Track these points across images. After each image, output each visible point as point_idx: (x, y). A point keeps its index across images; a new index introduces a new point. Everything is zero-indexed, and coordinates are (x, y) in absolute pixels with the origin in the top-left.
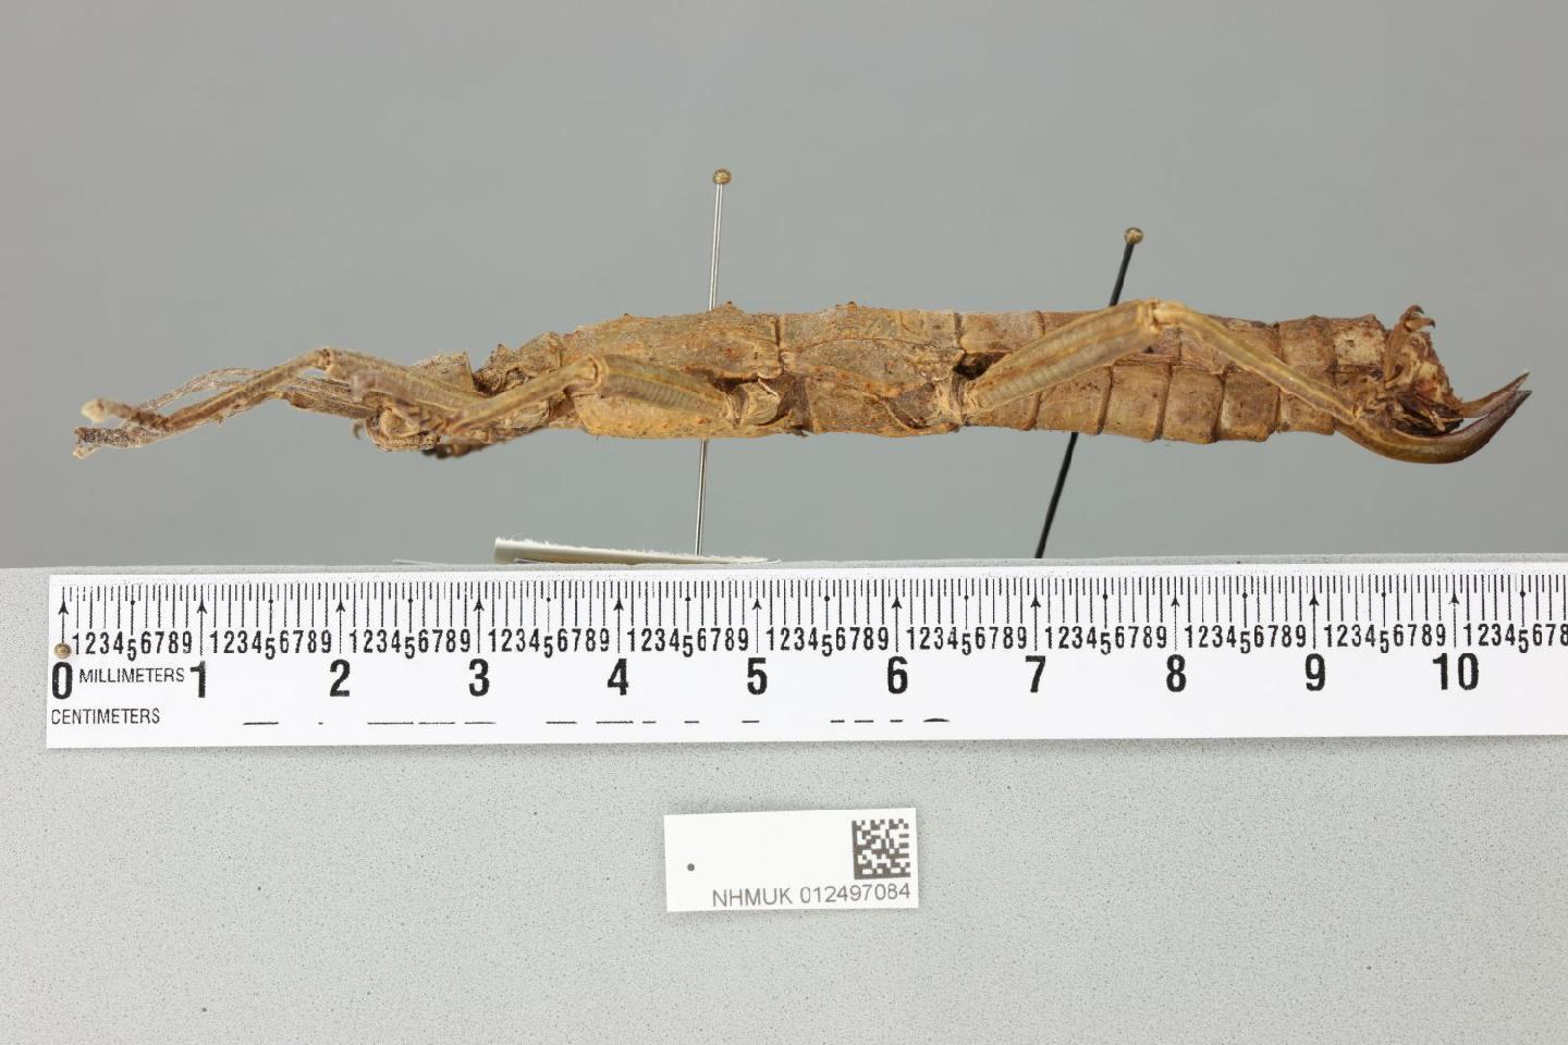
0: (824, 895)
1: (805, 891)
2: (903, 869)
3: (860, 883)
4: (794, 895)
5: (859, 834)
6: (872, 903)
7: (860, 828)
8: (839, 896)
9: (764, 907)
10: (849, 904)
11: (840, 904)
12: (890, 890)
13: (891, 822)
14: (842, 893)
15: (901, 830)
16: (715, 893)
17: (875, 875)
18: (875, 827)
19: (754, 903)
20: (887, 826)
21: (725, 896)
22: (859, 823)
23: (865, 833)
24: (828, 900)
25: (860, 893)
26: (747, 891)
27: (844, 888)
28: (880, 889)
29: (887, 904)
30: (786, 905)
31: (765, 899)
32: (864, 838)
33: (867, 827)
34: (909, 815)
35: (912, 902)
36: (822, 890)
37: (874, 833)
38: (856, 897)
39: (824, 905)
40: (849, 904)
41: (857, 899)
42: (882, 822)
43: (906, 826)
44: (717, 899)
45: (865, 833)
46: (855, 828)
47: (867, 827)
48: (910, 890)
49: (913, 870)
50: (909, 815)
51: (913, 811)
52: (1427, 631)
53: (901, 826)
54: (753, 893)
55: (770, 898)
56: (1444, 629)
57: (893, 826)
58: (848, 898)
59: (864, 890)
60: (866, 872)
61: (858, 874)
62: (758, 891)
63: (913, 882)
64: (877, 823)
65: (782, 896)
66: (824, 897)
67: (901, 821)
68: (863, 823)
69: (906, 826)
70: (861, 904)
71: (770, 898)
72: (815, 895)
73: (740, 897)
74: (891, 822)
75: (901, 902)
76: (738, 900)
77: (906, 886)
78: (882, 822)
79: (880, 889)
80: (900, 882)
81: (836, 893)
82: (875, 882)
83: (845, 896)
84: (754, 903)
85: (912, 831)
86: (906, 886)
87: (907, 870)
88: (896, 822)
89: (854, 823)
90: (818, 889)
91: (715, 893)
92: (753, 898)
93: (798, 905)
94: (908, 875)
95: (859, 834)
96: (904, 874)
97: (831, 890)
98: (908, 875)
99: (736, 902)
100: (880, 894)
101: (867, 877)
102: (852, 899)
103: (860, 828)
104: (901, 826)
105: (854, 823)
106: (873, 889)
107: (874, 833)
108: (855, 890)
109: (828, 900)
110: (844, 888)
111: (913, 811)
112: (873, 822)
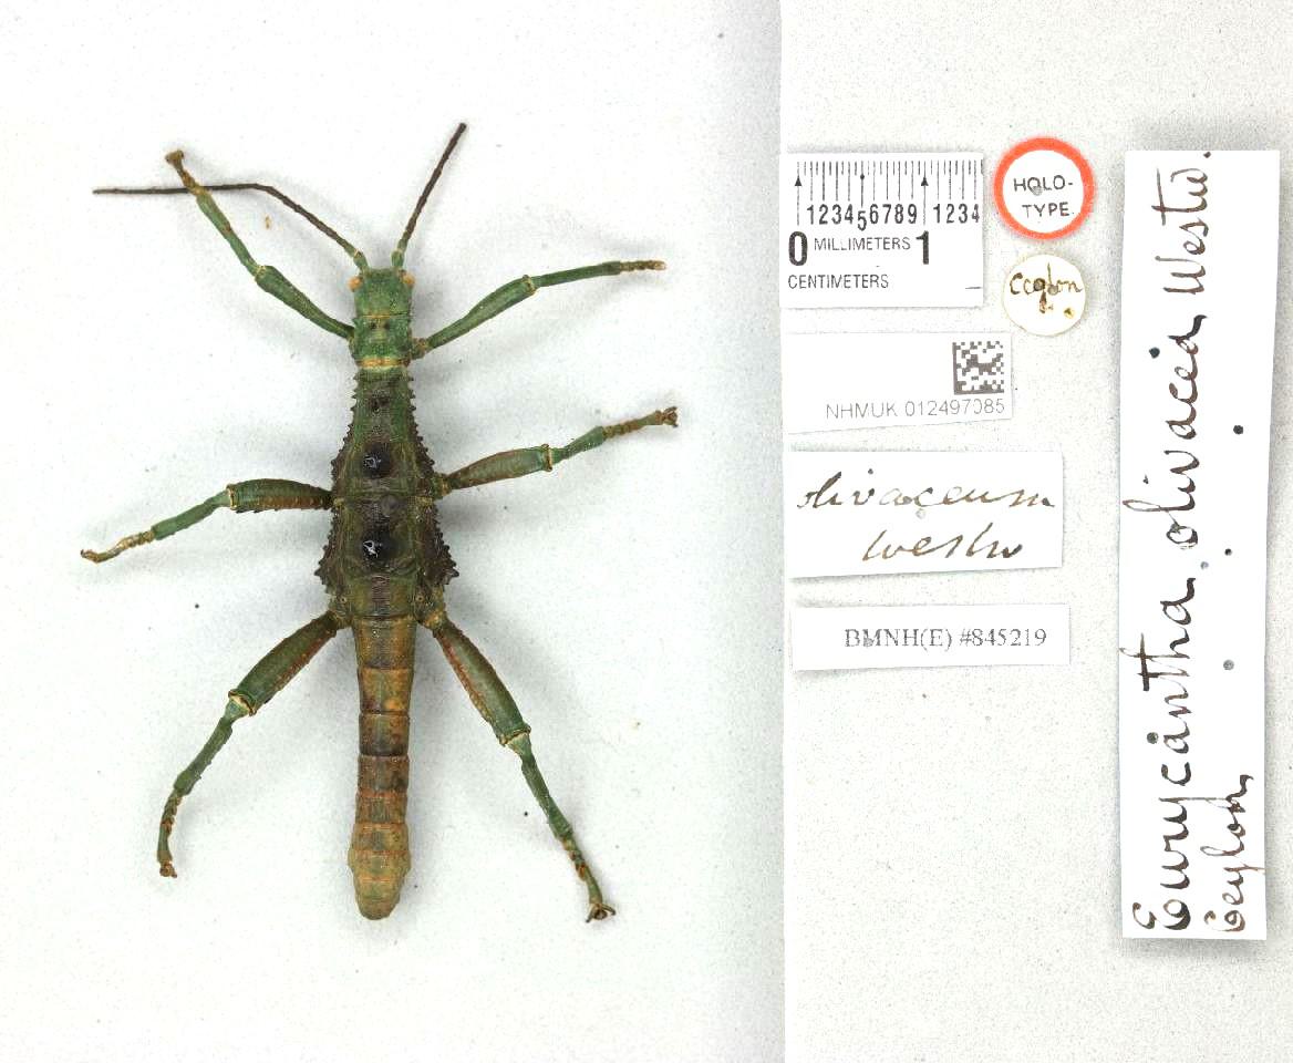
0: (927, 409)
4: (899, 408)
5: (959, 353)
7: (959, 348)
10: (950, 417)
20: (984, 346)
23: (965, 353)
32: (963, 356)
33: (967, 347)
37: (973, 352)
38: (955, 411)
45: (965, 353)
46: (955, 347)
47: (967, 347)
53: (997, 346)
57: (990, 346)
61: (958, 387)
72: (918, 409)
80: (994, 397)
81: (939, 406)
82: (972, 397)
88: (992, 344)
94: (1003, 391)
95: (959, 353)
96: (1000, 390)
97: (933, 405)
101: (968, 392)
103: (959, 348)
105: (954, 344)
107: (973, 352)
108: (955, 405)
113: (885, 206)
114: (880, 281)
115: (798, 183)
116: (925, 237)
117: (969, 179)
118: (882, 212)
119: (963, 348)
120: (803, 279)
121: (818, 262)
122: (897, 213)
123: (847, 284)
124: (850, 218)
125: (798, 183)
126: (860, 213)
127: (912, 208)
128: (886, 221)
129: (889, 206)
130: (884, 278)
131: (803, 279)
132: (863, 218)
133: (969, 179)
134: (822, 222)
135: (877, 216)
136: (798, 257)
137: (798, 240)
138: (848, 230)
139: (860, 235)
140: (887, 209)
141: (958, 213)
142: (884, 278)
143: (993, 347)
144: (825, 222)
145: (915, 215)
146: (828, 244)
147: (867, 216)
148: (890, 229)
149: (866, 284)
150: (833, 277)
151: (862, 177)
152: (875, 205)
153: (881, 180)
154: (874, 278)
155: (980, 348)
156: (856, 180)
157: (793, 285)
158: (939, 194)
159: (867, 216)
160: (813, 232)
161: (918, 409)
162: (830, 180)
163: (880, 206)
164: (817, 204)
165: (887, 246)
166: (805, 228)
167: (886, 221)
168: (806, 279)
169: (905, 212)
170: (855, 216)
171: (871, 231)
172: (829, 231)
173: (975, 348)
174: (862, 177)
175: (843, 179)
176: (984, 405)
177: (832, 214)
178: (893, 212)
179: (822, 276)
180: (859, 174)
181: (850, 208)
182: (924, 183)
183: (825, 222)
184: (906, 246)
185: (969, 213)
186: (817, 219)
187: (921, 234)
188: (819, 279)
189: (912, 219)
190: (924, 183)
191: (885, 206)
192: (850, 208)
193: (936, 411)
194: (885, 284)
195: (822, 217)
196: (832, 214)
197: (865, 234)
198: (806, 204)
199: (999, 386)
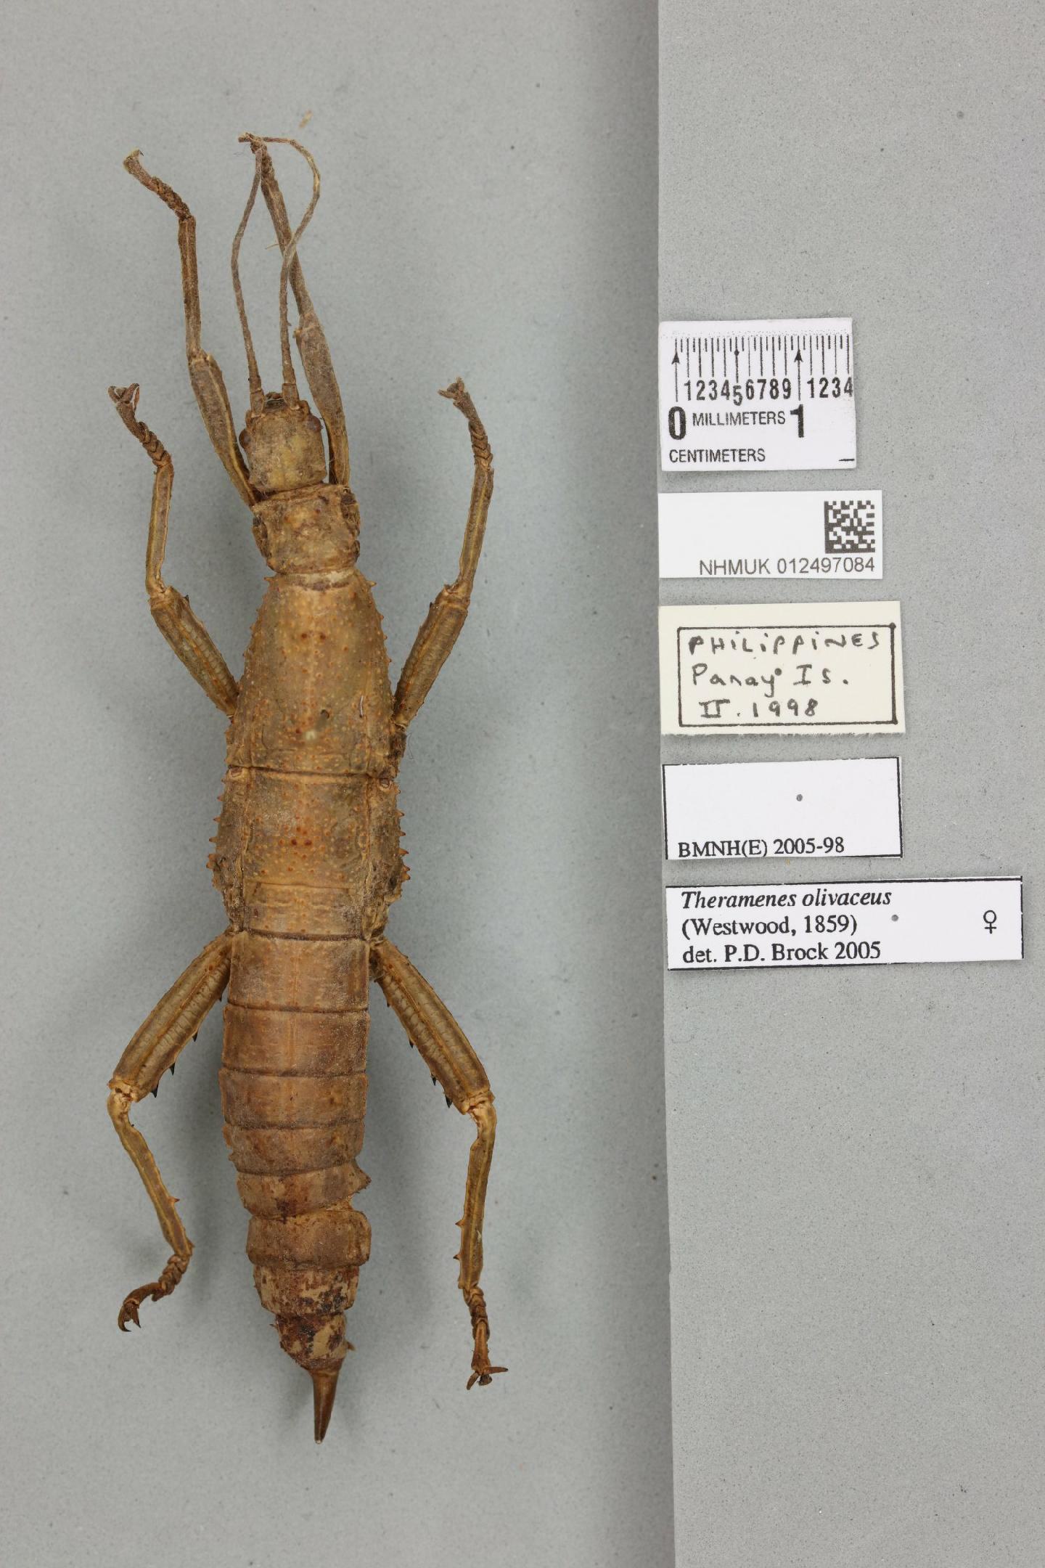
0: (799, 566)
1: (782, 562)
2: (869, 545)
3: (831, 556)
4: (772, 566)
5: (831, 513)
6: (841, 574)
8: (812, 568)
9: (745, 575)
11: (813, 574)
12: (857, 564)
13: (860, 503)
14: (815, 565)
15: (869, 510)
16: (702, 563)
17: (844, 550)
18: (844, 506)
19: (735, 573)
20: (855, 506)
21: (711, 565)
22: (830, 504)
23: (836, 512)
24: (801, 572)
25: (830, 565)
27: (817, 560)
28: (848, 562)
29: (854, 575)
30: (764, 574)
31: (746, 569)
32: (835, 517)
33: (838, 507)
34: (875, 497)
35: (877, 573)
37: (844, 512)
38: (826, 569)
40: (821, 575)
41: (827, 571)
42: (852, 503)
43: (873, 507)
44: (703, 567)
45: (836, 512)
46: (827, 507)
47: (838, 507)
48: (874, 564)
49: (878, 546)
52: (774, 386)
53: (868, 507)
54: (735, 565)
55: (751, 569)
56: (789, 383)
57: (861, 506)
58: (820, 570)
59: (834, 563)
60: (837, 547)
61: (829, 547)
62: (740, 562)
63: (878, 556)
64: (847, 503)
65: (760, 567)
66: (798, 569)
67: (868, 503)
68: (835, 503)
69: (873, 507)
70: (831, 575)
71: (751, 569)
72: (790, 566)
73: (724, 567)
74: (860, 503)
75: (867, 574)
76: (723, 569)
77: (871, 559)
78: (852, 503)
79: (848, 562)
80: (866, 557)
82: (843, 556)
83: (818, 568)
84: (735, 573)
85: (878, 511)
86: (871, 559)
87: (872, 546)
88: (864, 503)
89: (826, 504)
91: (702, 563)
92: (735, 568)
93: (775, 574)
94: (873, 550)
95: (831, 513)
96: (870, 549)
97: (804, 563)
98: (873, 550)
100: (848, 567)
102: (823, 571)
103: (831, 507)
105: (826, 504)
106: (842, 561)
107: (844, 512)
108: (826, 563)
109: (801, 572)
110: (817, 560)
112: (843, 503)
113: (759, 381)
115: (676, 360)
116: (799, 412)
119: (835, 507)
120: (682, 453)
121: (697, 437)
123: (726, 458)
124: (727, 395)
125: (676, 360)
128: (762, 397)
129: (764, 381)
130: (761, 452)
131: (682, 453)
132: (739, 394)
134: (700, 398)
137: (677, 415)
138: (723, 406)
139: (736, 410)
140: (761, 384)
141: (831, 387)
142: (761, 452)
143: (864, 507)
146: (704, 419)
148: (767, 404)
149: (743, 458)
150: (711, 451)
151: (737, 353)
152: (750, 381)
153: (755, 355)
154: (751, 452)
155: (852, 508)
156: (731, 356)
157: (674, 459)
159: (743, 391)
160: (691, 408)
161: (790, 566)
162: (706, 357)
163: (755, 381)
166: (683, 403)
167: (762, 397)
168: (686, 453)
169: (780, 387)
170: (731, 391)
171: (747, 405)
173: (847, 508)
174: (737, 353)
175: (719, 356)
176: (854, 564)
178: (768, 387)
179: (701, 451)
180: (734, 349)
181: (727, 383)
182: (798, 358)
186: (694, 395)
187: (796, 407)
188: (698, 454)
190: (798, 358)
191: (759, 381)
192: (727, 383)
193: (808, 569)
194: (761, 458)
195: (700, 393)
197: (741, 409)
198: (683, 379)
199: (869, 545)
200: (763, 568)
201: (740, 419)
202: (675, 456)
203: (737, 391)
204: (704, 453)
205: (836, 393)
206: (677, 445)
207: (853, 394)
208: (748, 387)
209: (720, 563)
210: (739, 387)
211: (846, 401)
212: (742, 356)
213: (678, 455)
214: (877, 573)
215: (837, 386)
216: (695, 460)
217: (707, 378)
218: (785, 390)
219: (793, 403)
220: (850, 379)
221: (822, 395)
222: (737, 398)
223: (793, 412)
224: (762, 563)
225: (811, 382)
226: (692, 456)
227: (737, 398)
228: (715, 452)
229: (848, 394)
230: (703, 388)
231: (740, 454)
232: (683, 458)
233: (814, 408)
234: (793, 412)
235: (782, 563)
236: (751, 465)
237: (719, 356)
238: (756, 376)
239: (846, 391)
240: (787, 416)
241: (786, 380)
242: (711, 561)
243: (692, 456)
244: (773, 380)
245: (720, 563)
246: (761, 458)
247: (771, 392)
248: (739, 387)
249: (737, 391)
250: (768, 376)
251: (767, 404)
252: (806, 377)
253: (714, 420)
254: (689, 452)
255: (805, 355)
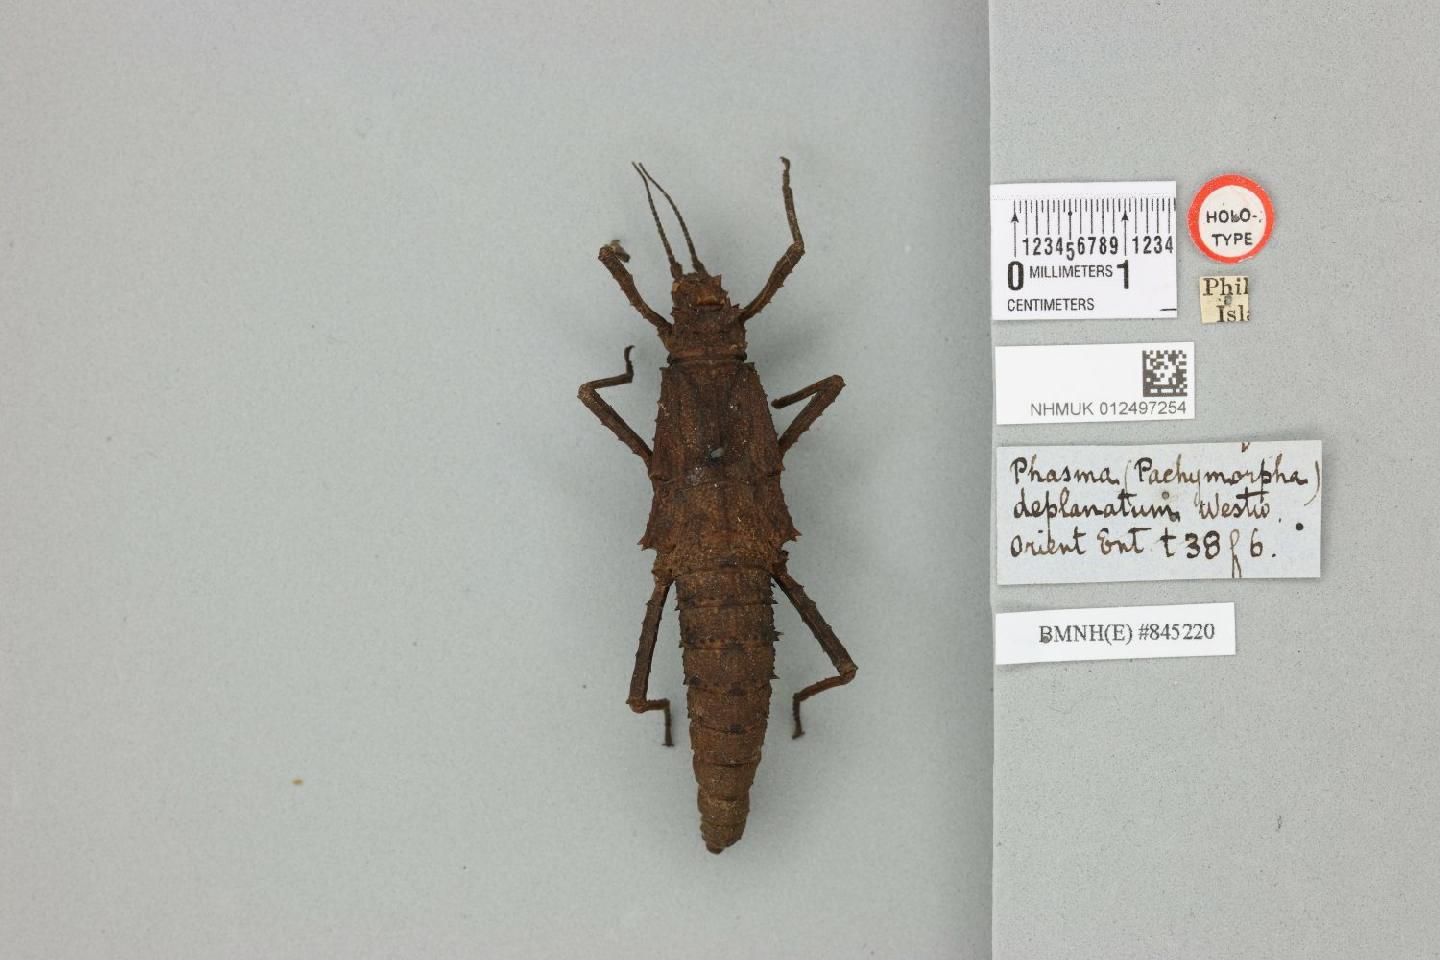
0: (1119, 409)
1: (1104, 406)
2: (1182, 390)
3: (1148, 399)
4: (1095, 408)
5: (1148, 361)
6: (1153, 415)
7: (1148, 357)
8: (1130, 410)
11: (1131, 416)
18: (1160, 356)
19: (1062, 414)
23: (1152, 361)
24: (1121, 413)
26: (1058, 405)
27: (1134, 404)
30: (1087, 418)
32: (1151, 364)
33: (1154, 356)
34: (1188, 348)
36: (1117, 406)
39: (1119, 418)
40: (1138, 417)
43: (1184, 356)
45: (1152, 361)
46: (1145, 356)
47: (1154, 356)
50: (1188, 348)
51: (1191, 345)
53: (1180, 356)
54: (1062, 407)
59: (1150, 406)
61: (1147, 393)
62: (1067, 405)
63: (1190, 401)
64: (1162, 353)
66: (1118, 411)
67: (1181, 352)
68: (1152, 353)
69: (1184, 356)
70: (1147, 417)
71: (1076, 411)
72: (1111, 409)
75: (1179, 415)
77: (1183, 403)
80: (1179, 400)
82: (1158, 399)
83: (1135, 410)
84: (1062, 414)
86: (1183, 403)
87: (1185, 391)
89: (1144, 353)
90: (1114, 405)
93: (1098, 417)
94: (1185, 394)
95: (1148, 361)
97: (1124, 406)
98: (1185, 394)
99: (1049, 412)
103: (1148, 357)
104: (1180, 356)
105: (1144, 353)
107: (1159, 360)
108: (1143, 406)
109: (1121, 413)
110: (1134, 404)
111: (1191, 345)
112: (1158, 352)
113: (1090, 239)
114: (1086, 304)
115: (1015, 219)
116: (1125, 266)
117: (1163, 216)
118: (1088, 244)
120: (1020, 302)
121: (1033, 288)
122: (1103, 244)
124: (1061, 250)
125: (1015, 219)
126: (1068, 244)
127: (1114, 241)
128: (1091, 253)
129: (1093, 239)
130: (1091, 301)
131: (1020, 302)
133: (1163, 216)
134: (1036, 253)
135: (1083, 247)
136: (1016, 283)
137: (1015, 268)
138: (1058, 260)
142: (1091, 301)
144: (1039, 253)
145: (1116, 246)
146: (1040, 272)
147: (1075, 247)
148: (1096, 259)
149: (1074, 307)
151: (1070, 214)
153: (1086, 216)
154: (1082, 302)
156: (1064, 216)
158: (1138, 227)
159: (1075, 247)
160: (1029, 261)
161: (1111, 409)
163: (1086, 238)
164: (1032, 236)
165: (1092, 274)
167: (1091, 253)
168: (1022, 302)
169: (1107, 244)
170: (1064, 246)
171: (1079, 260)
172: (1042, 260)
173: (1161, 356)
174: (1070, 214)
175: (1054, 216)
177: (1044, 246)
178: (1098, 244)
179: (1036, 300)
180: (1067, 211)
181: (1060, 240)
182: (1125, 218)
183: (1039, 253)
184: (1109, 274)
185: (1163, 244)
186: (1031, 251)
187: (1122, 262)
188: (1033, 302)
189: (1114, 250)
190: (1125, 218)
191: (1090, 239)
192: (1060, 240)
195: (1036, 249)
196: (1044, 246)
197: (1073, 263)
198: (1021, 236)
199: (1182, 390)
200: (1087, 410)
201: (1073, 272)
202: (1012, 305)
203: (1070, 247)
204: (1039, 303)
205: (1158, 249)
206: (1016, 295)
207: (1174, 251)
208: (1079, 243)
209: (1049, 406)
210: (1072, 243)
211: (1168, 259)
212: (1075, 216)
213: (1015, 304)
214: (1190, 414)
215: (1159, 243)
216: (1031, 308)
217: (1043, 236)
218: (1112, 246)
219: (1120, 258)
220: (1170, 239)
221: (1146, 252)
222: (1070, 253)
223: (1119, 266)
224: (1086, 405)
225: (1136, 240)
226: (1029, 305)
227: (1070, 253)
228: (1049, 302)
229: (1168, 251)
230: (1039, 243)
231: (1071, 303)
232: (1020, 307)
233: (1137, 262)
234: (1119, 266)
235: (1104, 406)
236: (1082, 314)
237: (1054, 216)
238: (1086, 234)
239: (1167, 248)
240: (1115, 269)
241: (1113, 238)
242: (1040, 405)
243: (1029, 305)
244: (1103, 238)
245: (1049, 406)
246: (1091, 307)
247: (1101, 248)
248: (1072, 243)
249: (1070, 247)
250: (1098, 235)
251: (1096, 259)
252: (1131, 236)
253: (1049, 273)
254: (1026, 301)
255: (1131, 216)
